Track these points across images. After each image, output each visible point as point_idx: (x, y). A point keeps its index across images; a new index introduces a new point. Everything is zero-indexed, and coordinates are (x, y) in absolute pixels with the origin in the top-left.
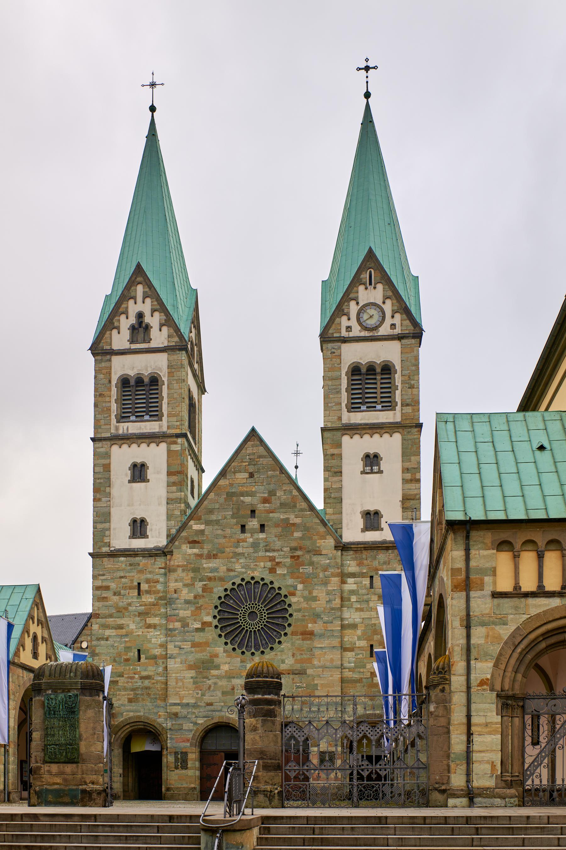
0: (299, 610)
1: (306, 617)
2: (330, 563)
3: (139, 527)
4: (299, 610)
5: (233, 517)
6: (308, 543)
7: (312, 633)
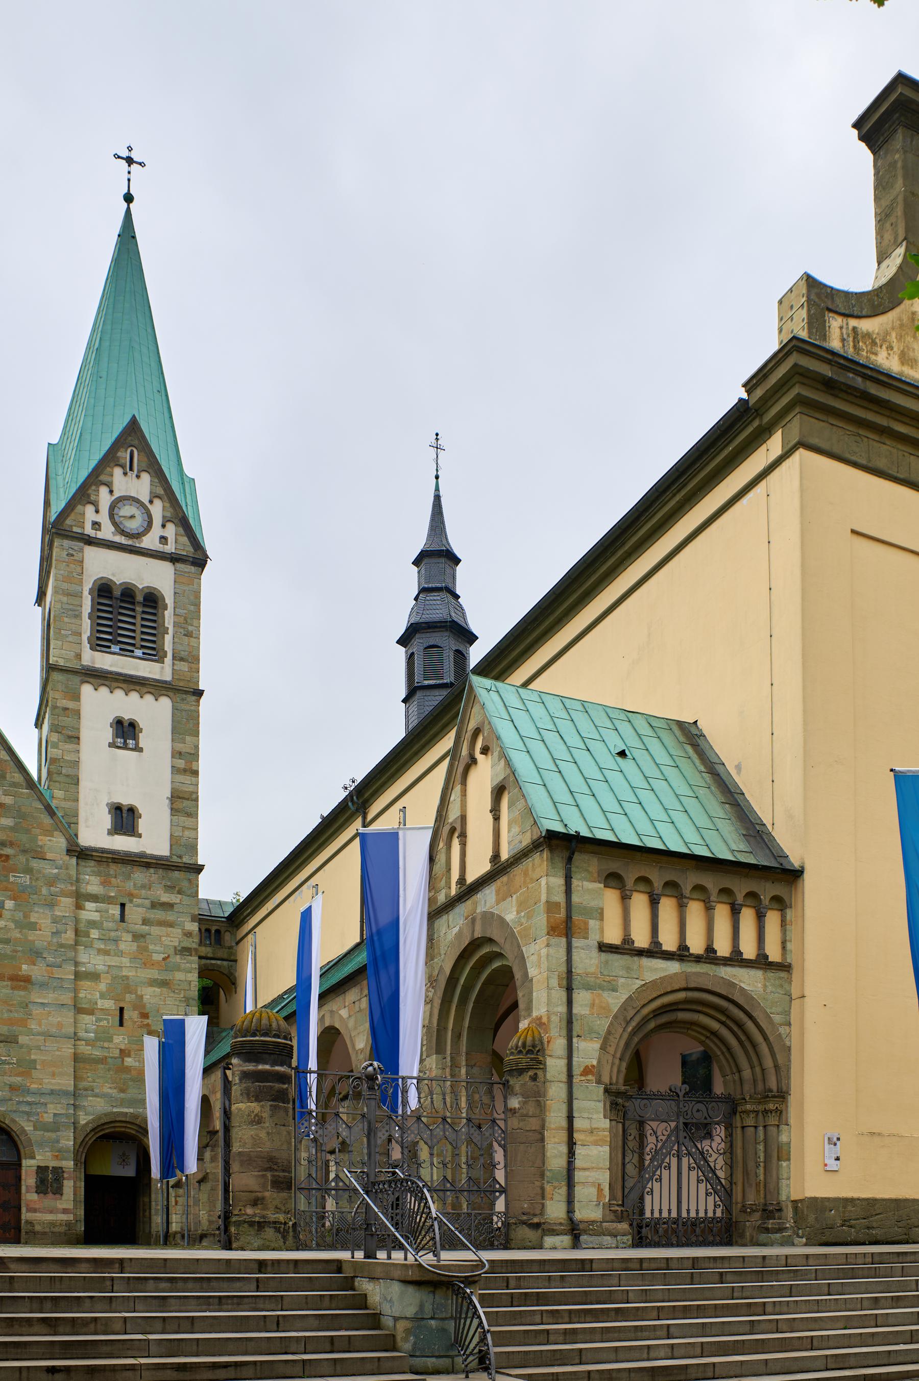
1: (19, 954)
2: (58, 874)
6: (24, 838)
7: (27, 980)
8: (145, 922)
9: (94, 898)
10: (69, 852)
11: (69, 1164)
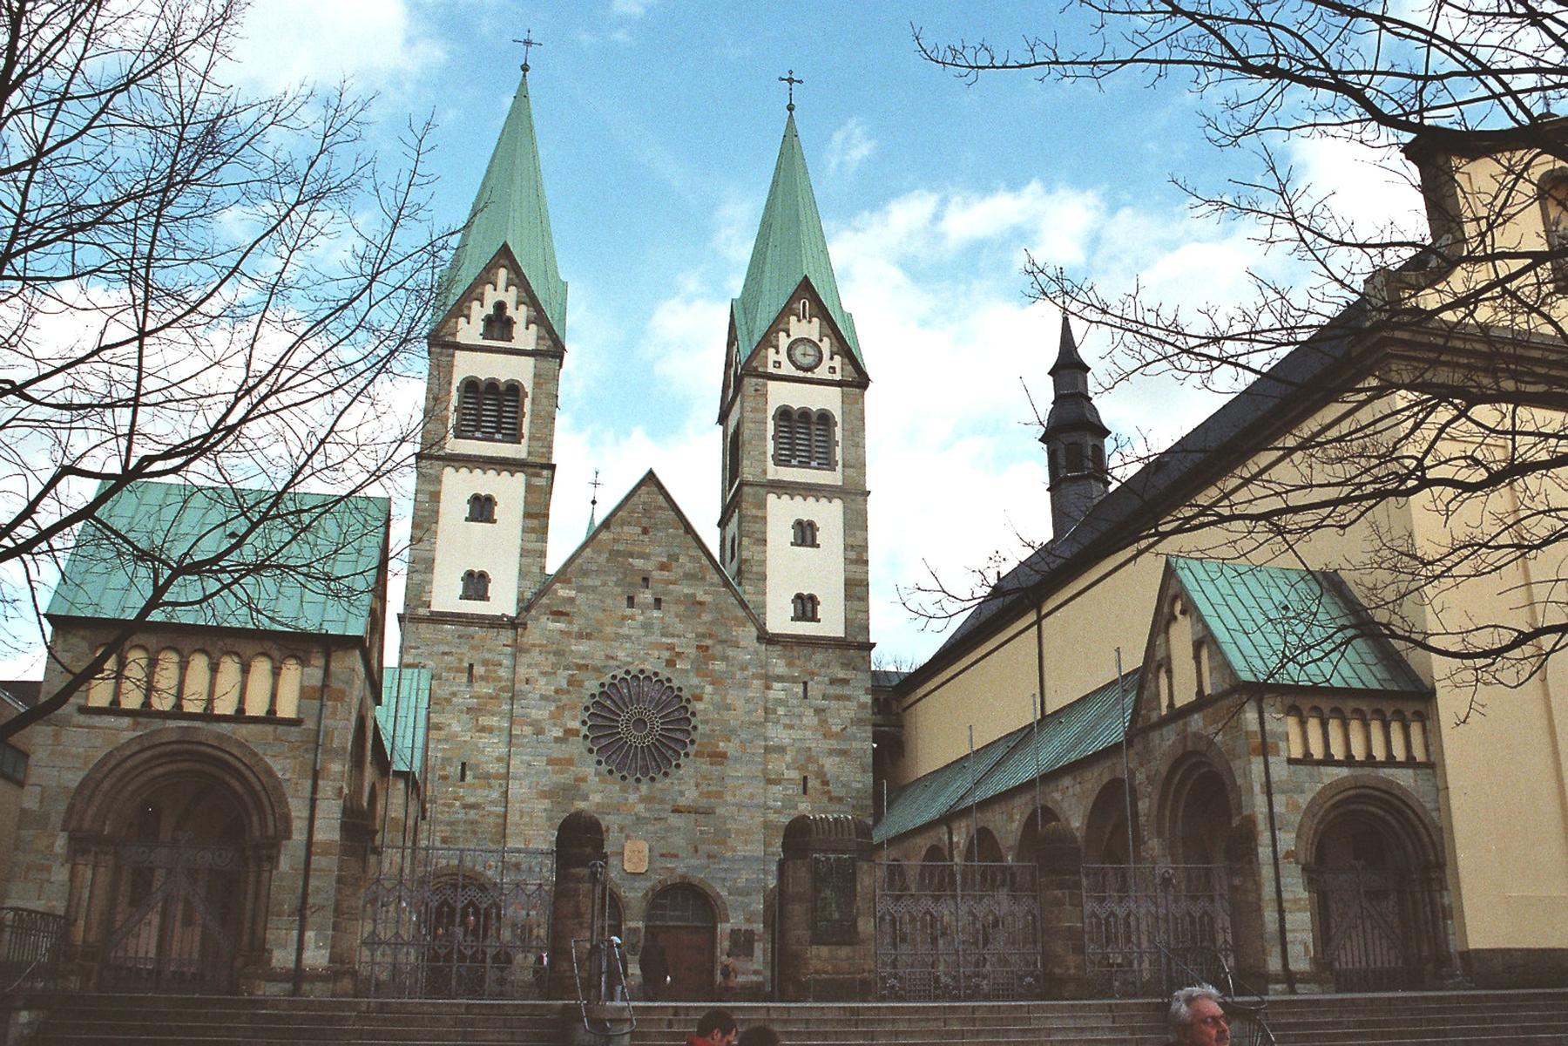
0: (706, 722)
3: (476, 584)
4: (706, 722)
5: (617, 584)
7: (724, 756)
8: (824, 697)
9: (780, 679)
10: (759, 639)
11: (759, 927)
